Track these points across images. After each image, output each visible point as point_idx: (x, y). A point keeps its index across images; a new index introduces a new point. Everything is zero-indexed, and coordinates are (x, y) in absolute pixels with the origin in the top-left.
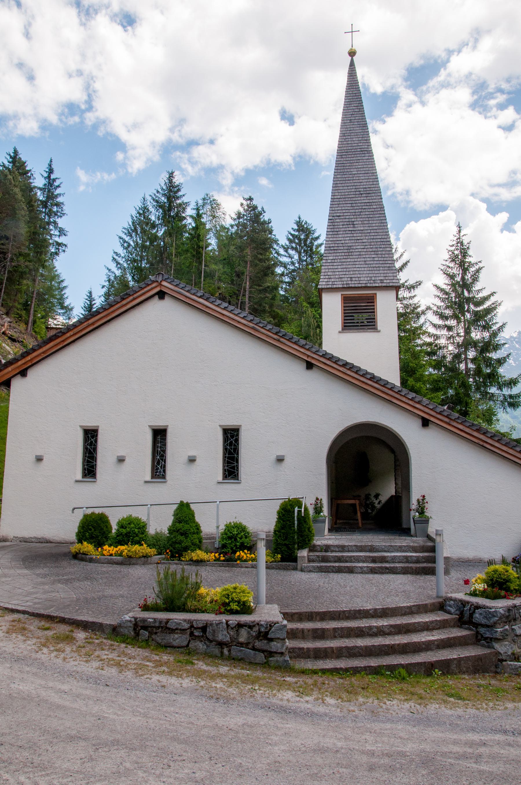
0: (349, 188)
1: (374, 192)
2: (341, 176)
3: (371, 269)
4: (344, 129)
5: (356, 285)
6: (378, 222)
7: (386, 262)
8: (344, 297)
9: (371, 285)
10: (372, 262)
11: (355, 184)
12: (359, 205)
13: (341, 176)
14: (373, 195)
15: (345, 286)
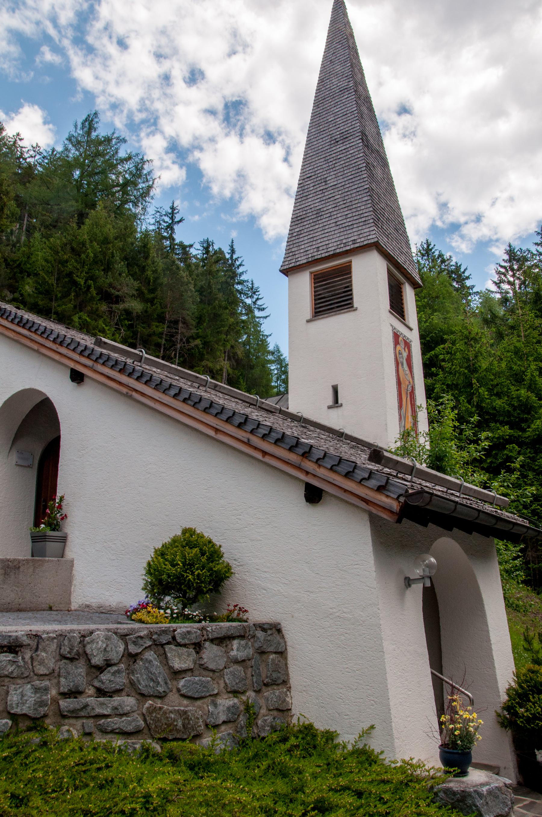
0: (324, 139)
1: (352, 134)
2: (316, 129)
3: (342, 230)
4: (324, 74)
5: (323, 255)
6: (355, 168)
7: (362, 216)
8: (315, 275)
9: (341, 250)
10: (345, 221)
11: (331, 133)
12: (333, 155)
13: (316, 129)
14: (351, 138)
15: (310, 260)
